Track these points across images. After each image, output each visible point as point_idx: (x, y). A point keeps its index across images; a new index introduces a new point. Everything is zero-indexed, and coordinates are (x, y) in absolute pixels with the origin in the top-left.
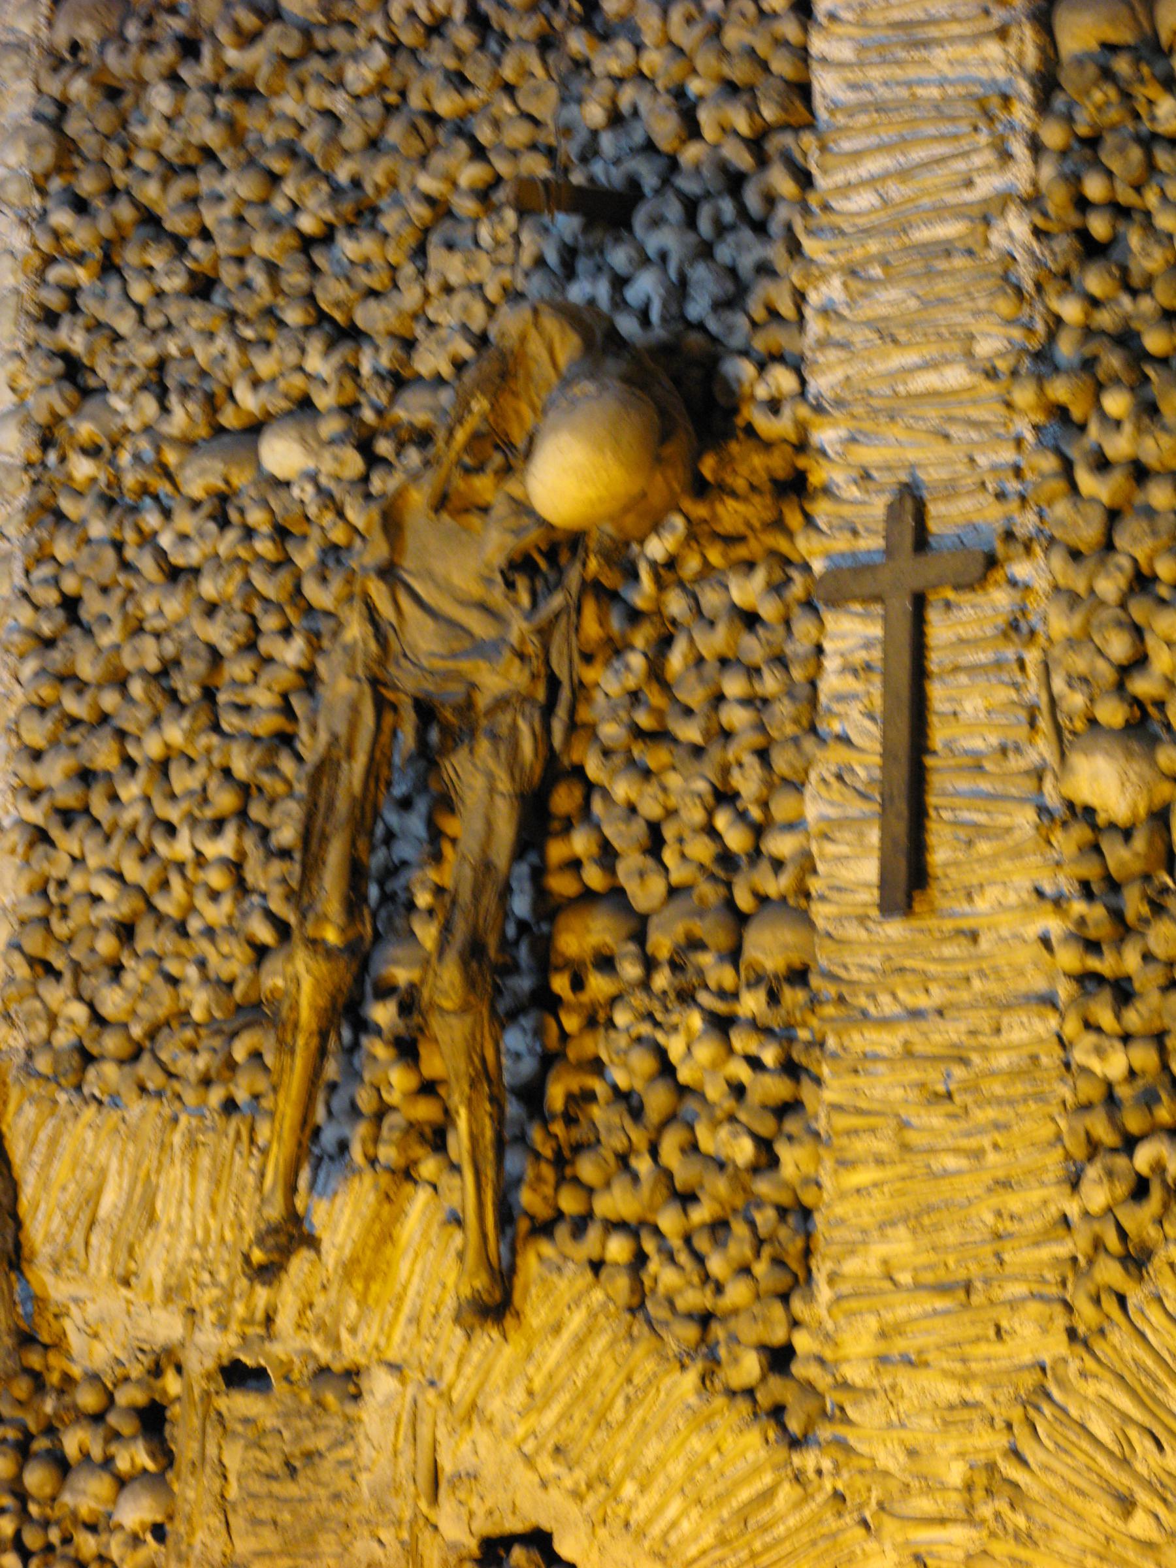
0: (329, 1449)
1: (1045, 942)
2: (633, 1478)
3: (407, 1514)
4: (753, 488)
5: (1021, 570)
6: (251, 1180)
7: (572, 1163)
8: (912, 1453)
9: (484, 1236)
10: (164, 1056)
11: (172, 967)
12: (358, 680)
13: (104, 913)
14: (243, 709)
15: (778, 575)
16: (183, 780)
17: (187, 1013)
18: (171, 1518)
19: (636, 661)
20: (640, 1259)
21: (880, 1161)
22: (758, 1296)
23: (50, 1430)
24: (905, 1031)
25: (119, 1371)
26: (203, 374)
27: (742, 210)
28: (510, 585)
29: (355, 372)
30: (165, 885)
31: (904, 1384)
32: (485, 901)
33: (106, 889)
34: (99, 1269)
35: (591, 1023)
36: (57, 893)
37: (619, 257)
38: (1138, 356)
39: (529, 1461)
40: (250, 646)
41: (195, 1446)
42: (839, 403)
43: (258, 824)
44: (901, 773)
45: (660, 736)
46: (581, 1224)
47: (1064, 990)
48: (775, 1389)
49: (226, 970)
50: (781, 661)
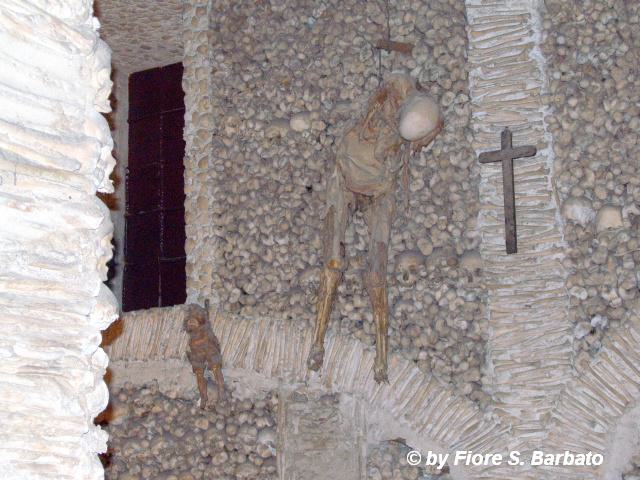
4: (456, 130)
11: (269, 277)
13: (244, 262)
14: (288, 200)
16: (269, 222)
19: (420, 181)
21: (508, 327)
22: (470, 367)
23: (232, 414)
24: (515, 288)
30: (266, 253)
33: (246, 255)
38: (578, 90)
42: (483, 104)
44: (510, 212)
45: (430, 202)
46: (411, 347)
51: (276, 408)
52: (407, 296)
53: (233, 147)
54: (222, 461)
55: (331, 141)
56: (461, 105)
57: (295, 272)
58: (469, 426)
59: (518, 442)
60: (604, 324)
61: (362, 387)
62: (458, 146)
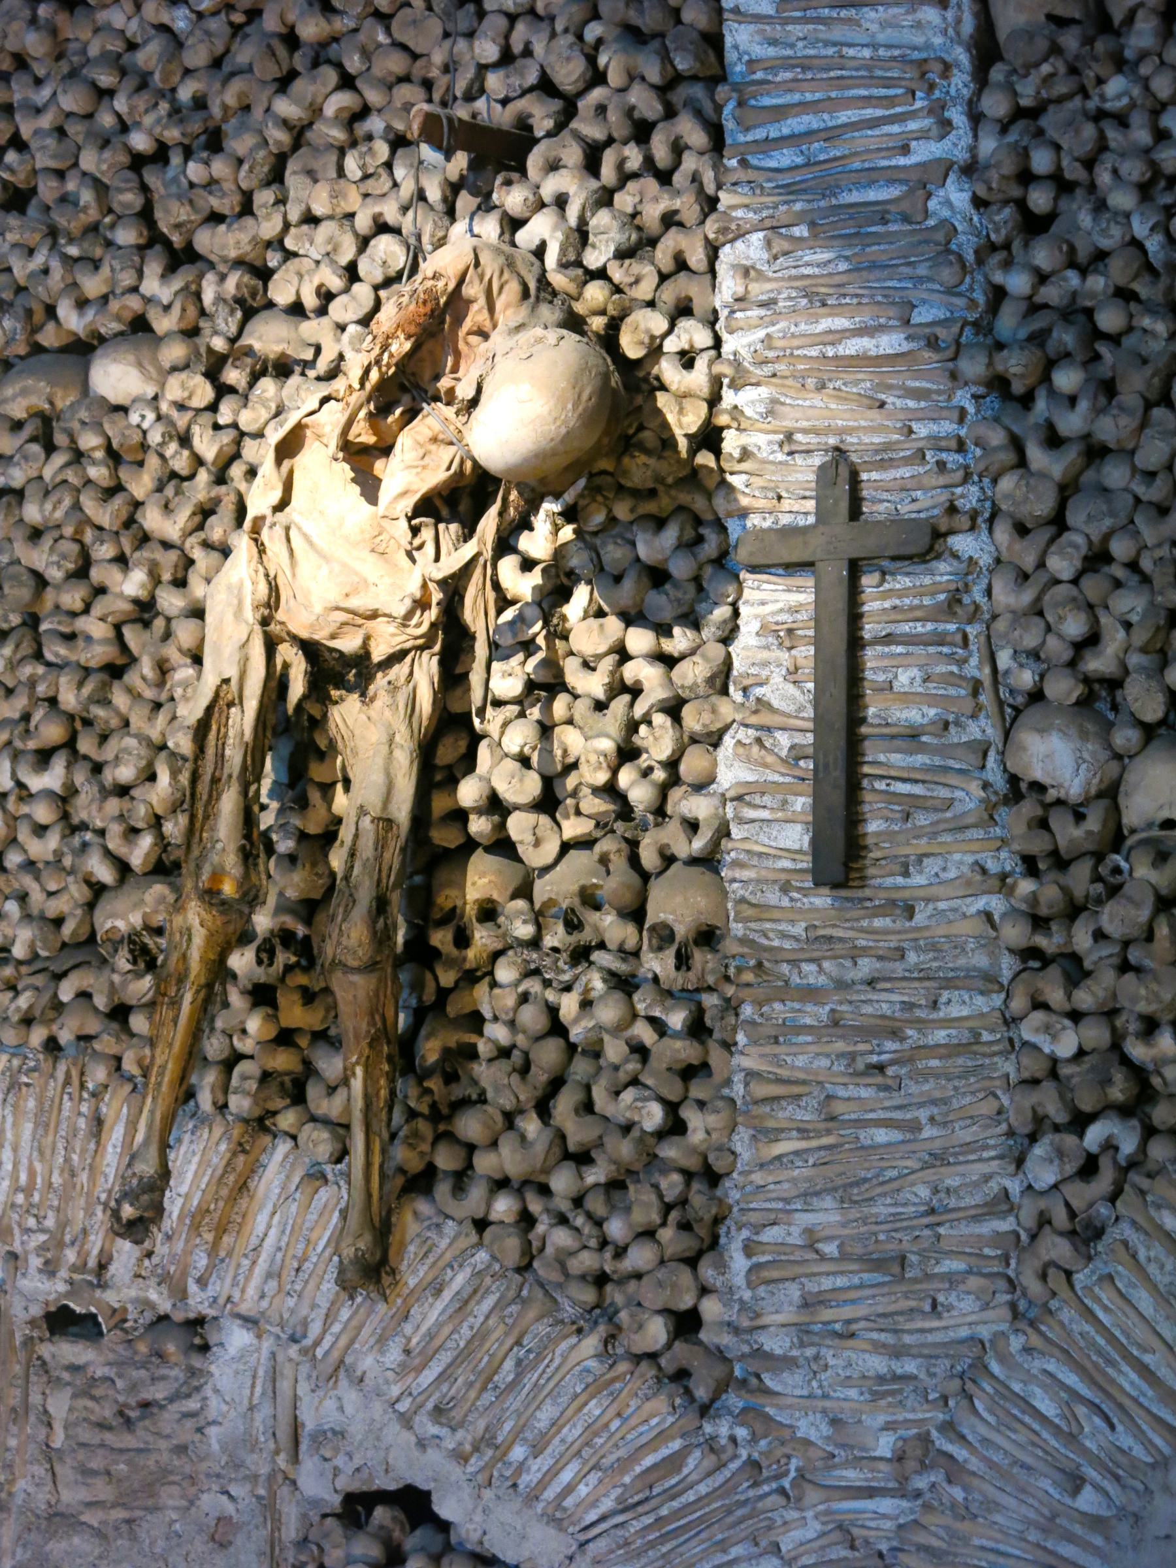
0: (171, 1400)
1: (988, 916)
2: (525, 1440)
3: (264, 1470)
5: (963, 544)
6: (82, 1123)
7: (449, 1118)
8: (835, 1422)
9: (369, 1195)
15: (689, 534)
20: (527, 1220)
21: (804, 1132)
22: (662, 1262)
26: (20, 290)
27: (649, 161)
29: (198, 296)
31: (828, 1354)
32: (387, 855)
37: (514, 199)
39: (406, 1421)
40: (81, 572)
41: (18, 1392)
43: (86, 757)
47: (1007, 966)
49: (54, 908)
56: (687, 359)
57: (78, 892)
58: (649, 1461)
59: (813, 1528)
60: (1128, 1145)
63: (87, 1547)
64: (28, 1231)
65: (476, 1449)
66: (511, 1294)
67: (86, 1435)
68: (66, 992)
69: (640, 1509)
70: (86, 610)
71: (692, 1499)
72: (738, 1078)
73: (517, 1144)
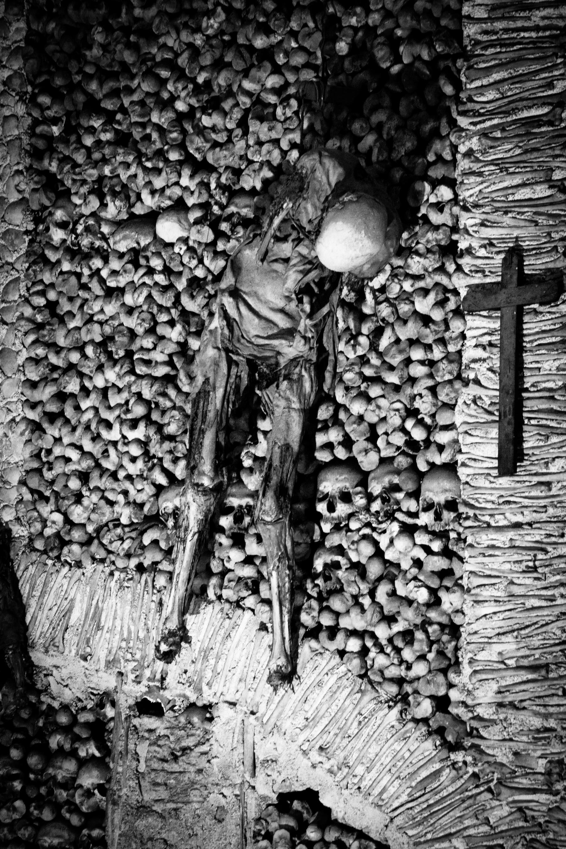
0: (196, 746)
3: (239, 781)
6: (153, 605)
7: (327, 599)
9: (284, 639)
10: (105, 541)
11: (111, 496)
12: (218, 348)
13: (72, 467)
14: (148, 363)
15: (441, 297)
16: (114, 399)
17: (118, 520)
18: (109, 781)
22: (430, 671)
24: (511, 534)
25: (80, 704)
28: (300, 301)
33: (74, 455)
34: (70, 651)
35: (337, 528)
36: (46, 457)
41: (122, 743)
43: (156, 423)
45: (377, 380)
46: (333, 632)
48: (440, 720)
49: (140, 498)
50: (442, 341)
51: (112, 724)
52: (334, 540)
53: (59, 262)
54: (16, 816)
55: (221, 263)
56: (439, 207)
58: (424, 774)
59: (506, 810)
61: (251, 694)
62: (428, 282)
63: (156, 823)
64: (127, 660)
65: (340, 769)
66: (357, 688)
67: (156, 765)
68: (147, 540)
69: (420, 800)
70: (154, 348)
71: (445, 794)
72: (465, 576)
73: (359, 611)
